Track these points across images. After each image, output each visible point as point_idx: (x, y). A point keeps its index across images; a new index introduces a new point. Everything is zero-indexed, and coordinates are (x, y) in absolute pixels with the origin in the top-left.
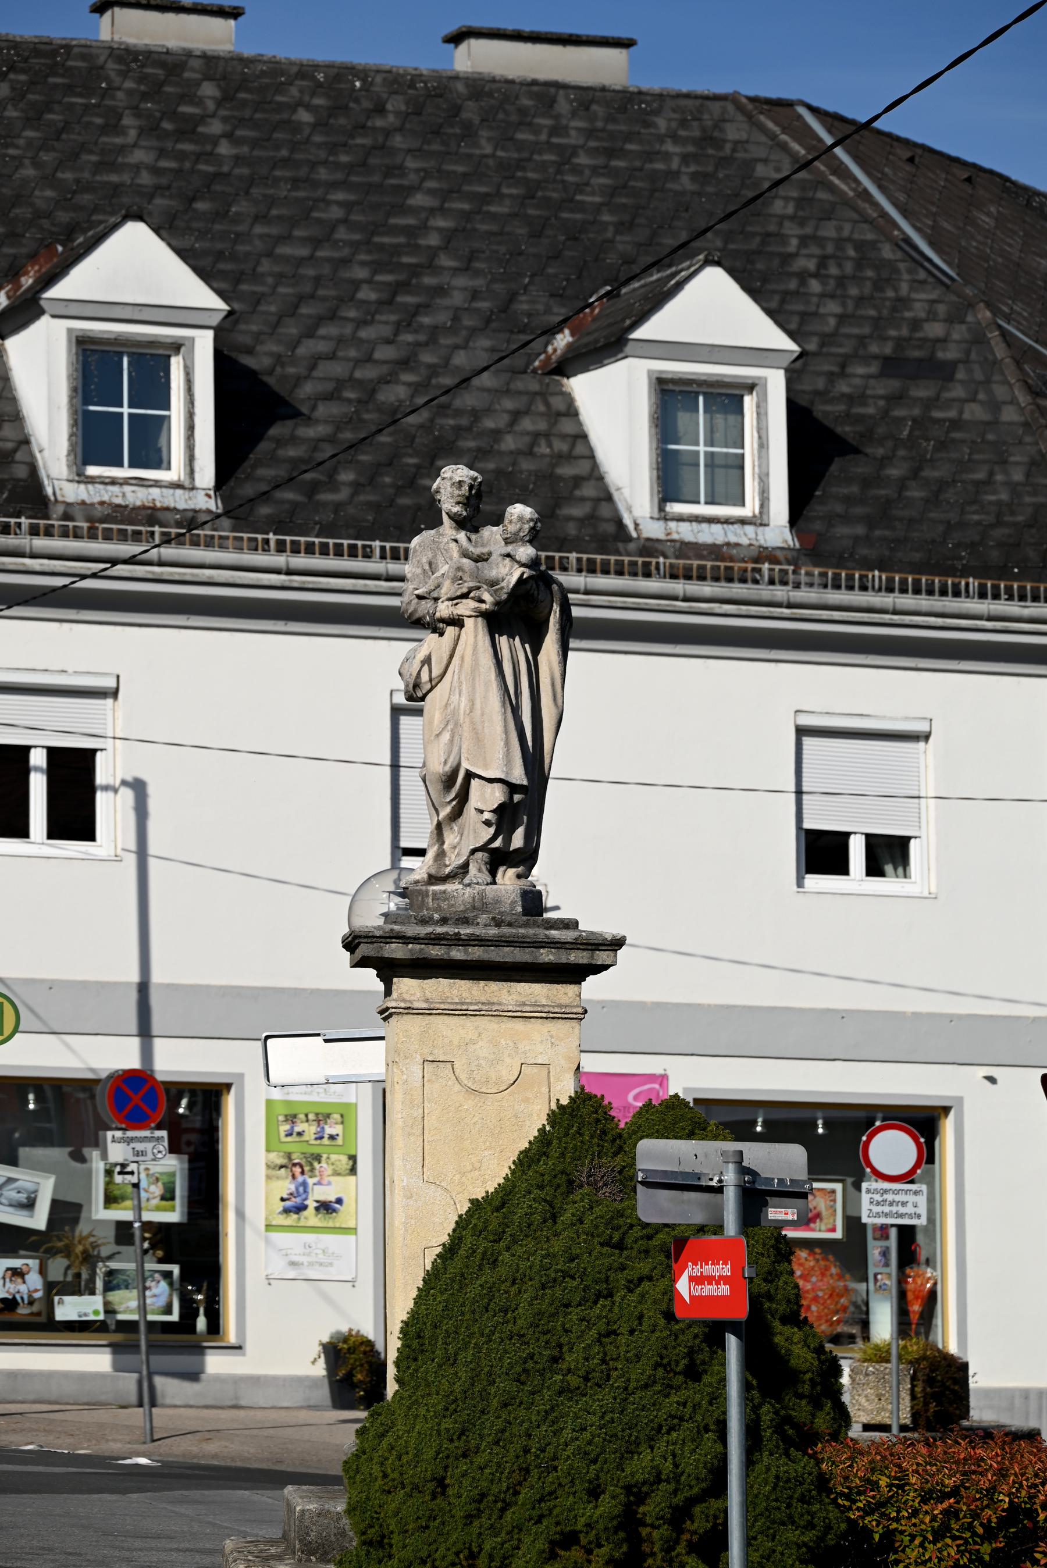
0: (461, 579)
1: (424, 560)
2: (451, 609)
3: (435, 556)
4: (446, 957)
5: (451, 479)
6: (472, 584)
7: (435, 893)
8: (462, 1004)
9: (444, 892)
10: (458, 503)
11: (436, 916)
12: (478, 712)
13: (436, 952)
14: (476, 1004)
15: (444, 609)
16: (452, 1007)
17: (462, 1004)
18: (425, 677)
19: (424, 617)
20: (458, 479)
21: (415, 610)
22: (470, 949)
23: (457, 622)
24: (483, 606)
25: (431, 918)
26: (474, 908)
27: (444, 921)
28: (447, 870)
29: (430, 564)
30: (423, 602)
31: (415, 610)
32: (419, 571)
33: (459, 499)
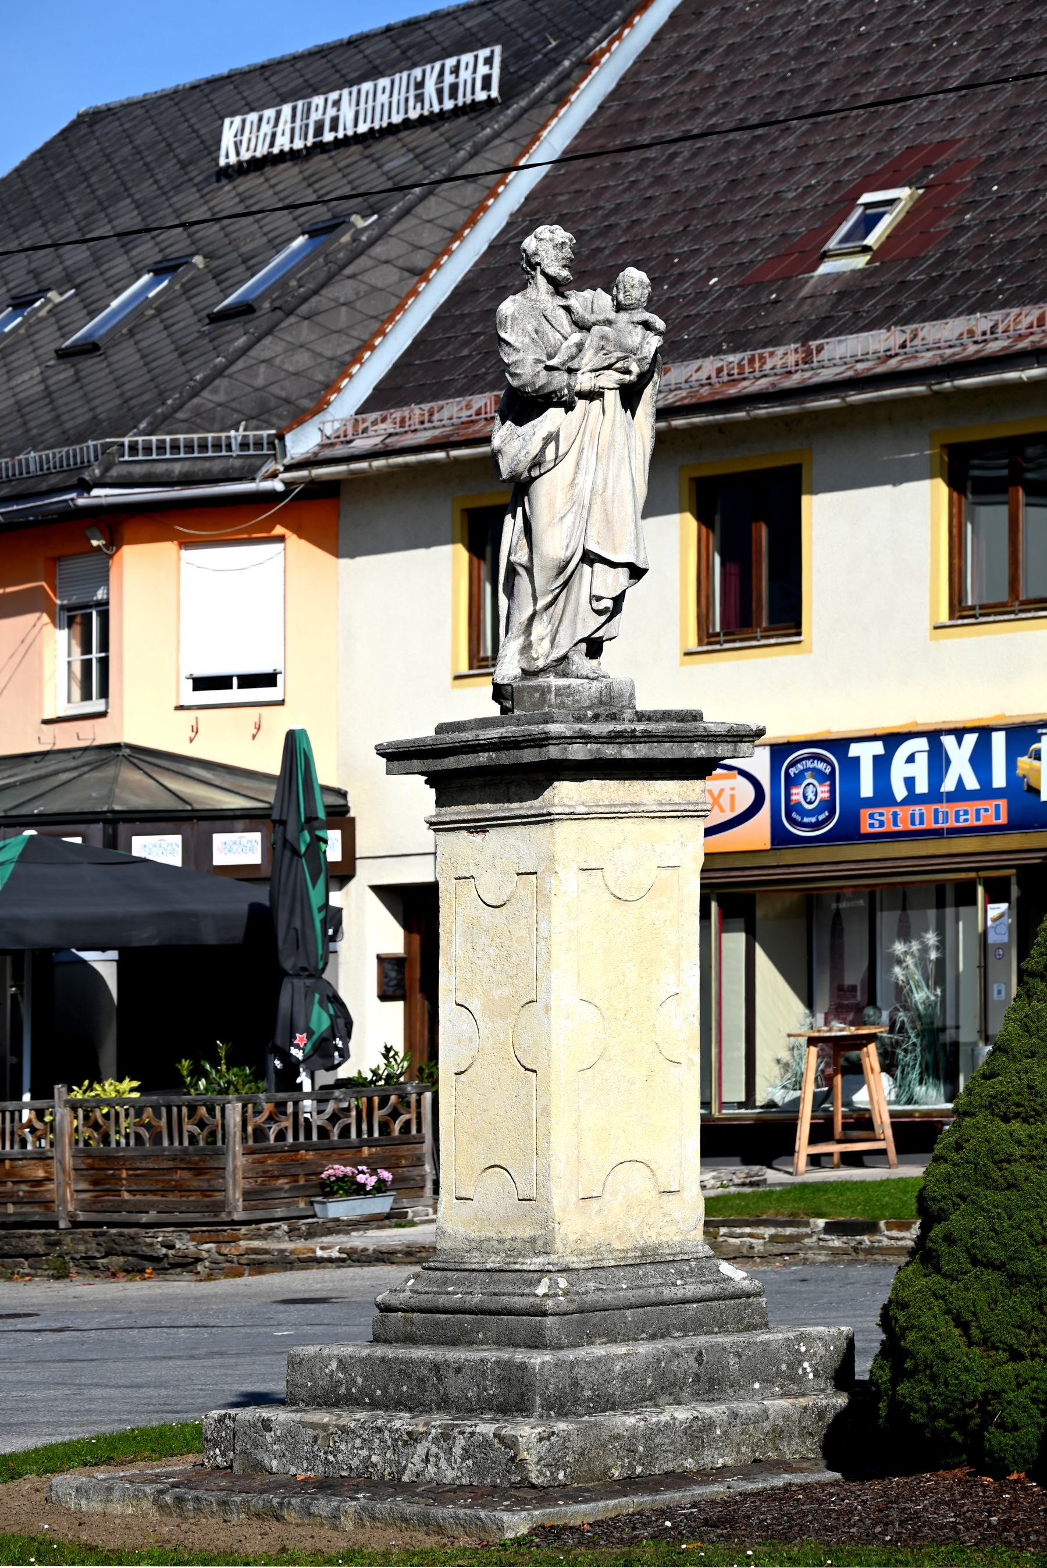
0: (603, 348)
1: (530, 328)
2: (594, 381)
3: (540, 324)
4: (618, 756)
5: (551, 240)
6: (620, 354)
7: (558, 689)
8: (611, 805)
9: (569, 687)
10: (564, 266)
11: (590, 713)
12: (609, 492)
13: (610, 751)
14: (625, 805)
15: (584, 381)
16: (607, 810)
17: (615, 806)
18: (550, 453)
19: (561, 390)
20: (561, 240)
21: (549, 383)
22: (638, 747)
23: (593, 395)
24: (627, 378)
25: (585, 715)
26: (601, 702)
27: (596, 717)
28: (541, 663)
29: (537, 332)
30: (556, 374)
31: (549, 383)
32: (527, 340)
33: (564, 262)
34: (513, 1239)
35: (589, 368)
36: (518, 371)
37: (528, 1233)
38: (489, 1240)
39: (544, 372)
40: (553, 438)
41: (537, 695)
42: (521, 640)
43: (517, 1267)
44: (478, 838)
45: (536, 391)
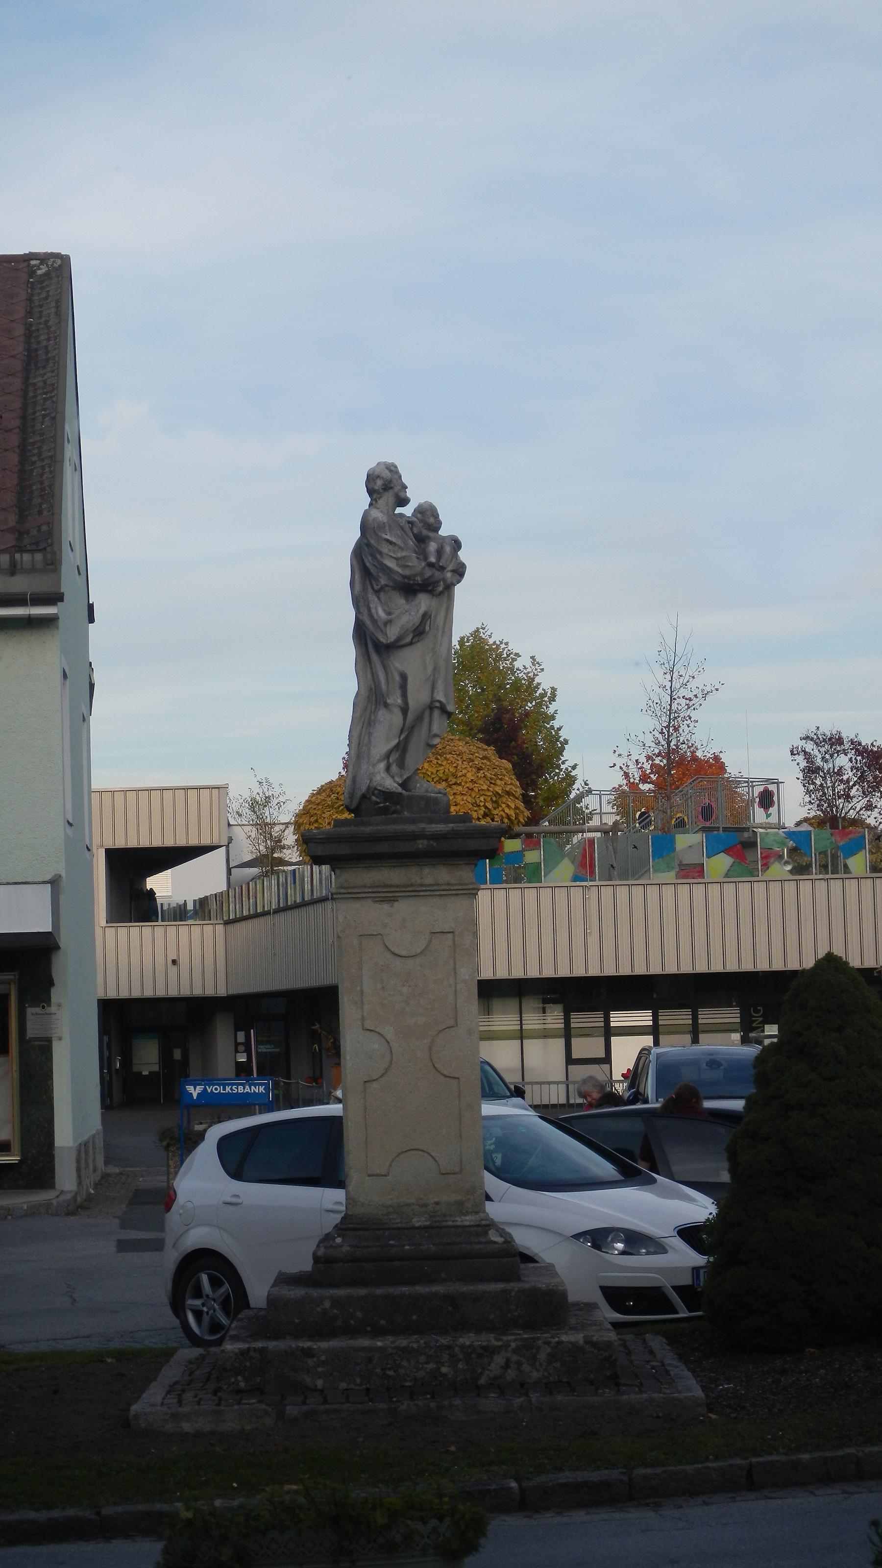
19: (438, 582)
34: (437, 1203)
35: (450, 568)
36: (410, 564)
37: (454, 1198)
38: (408, 1205)
39: (427, 568)
40: (426, 616)
41: (423, 803)
42: (385, 762)
43: (450, 1223)
44: (386, 907)
45: (424, 580)
